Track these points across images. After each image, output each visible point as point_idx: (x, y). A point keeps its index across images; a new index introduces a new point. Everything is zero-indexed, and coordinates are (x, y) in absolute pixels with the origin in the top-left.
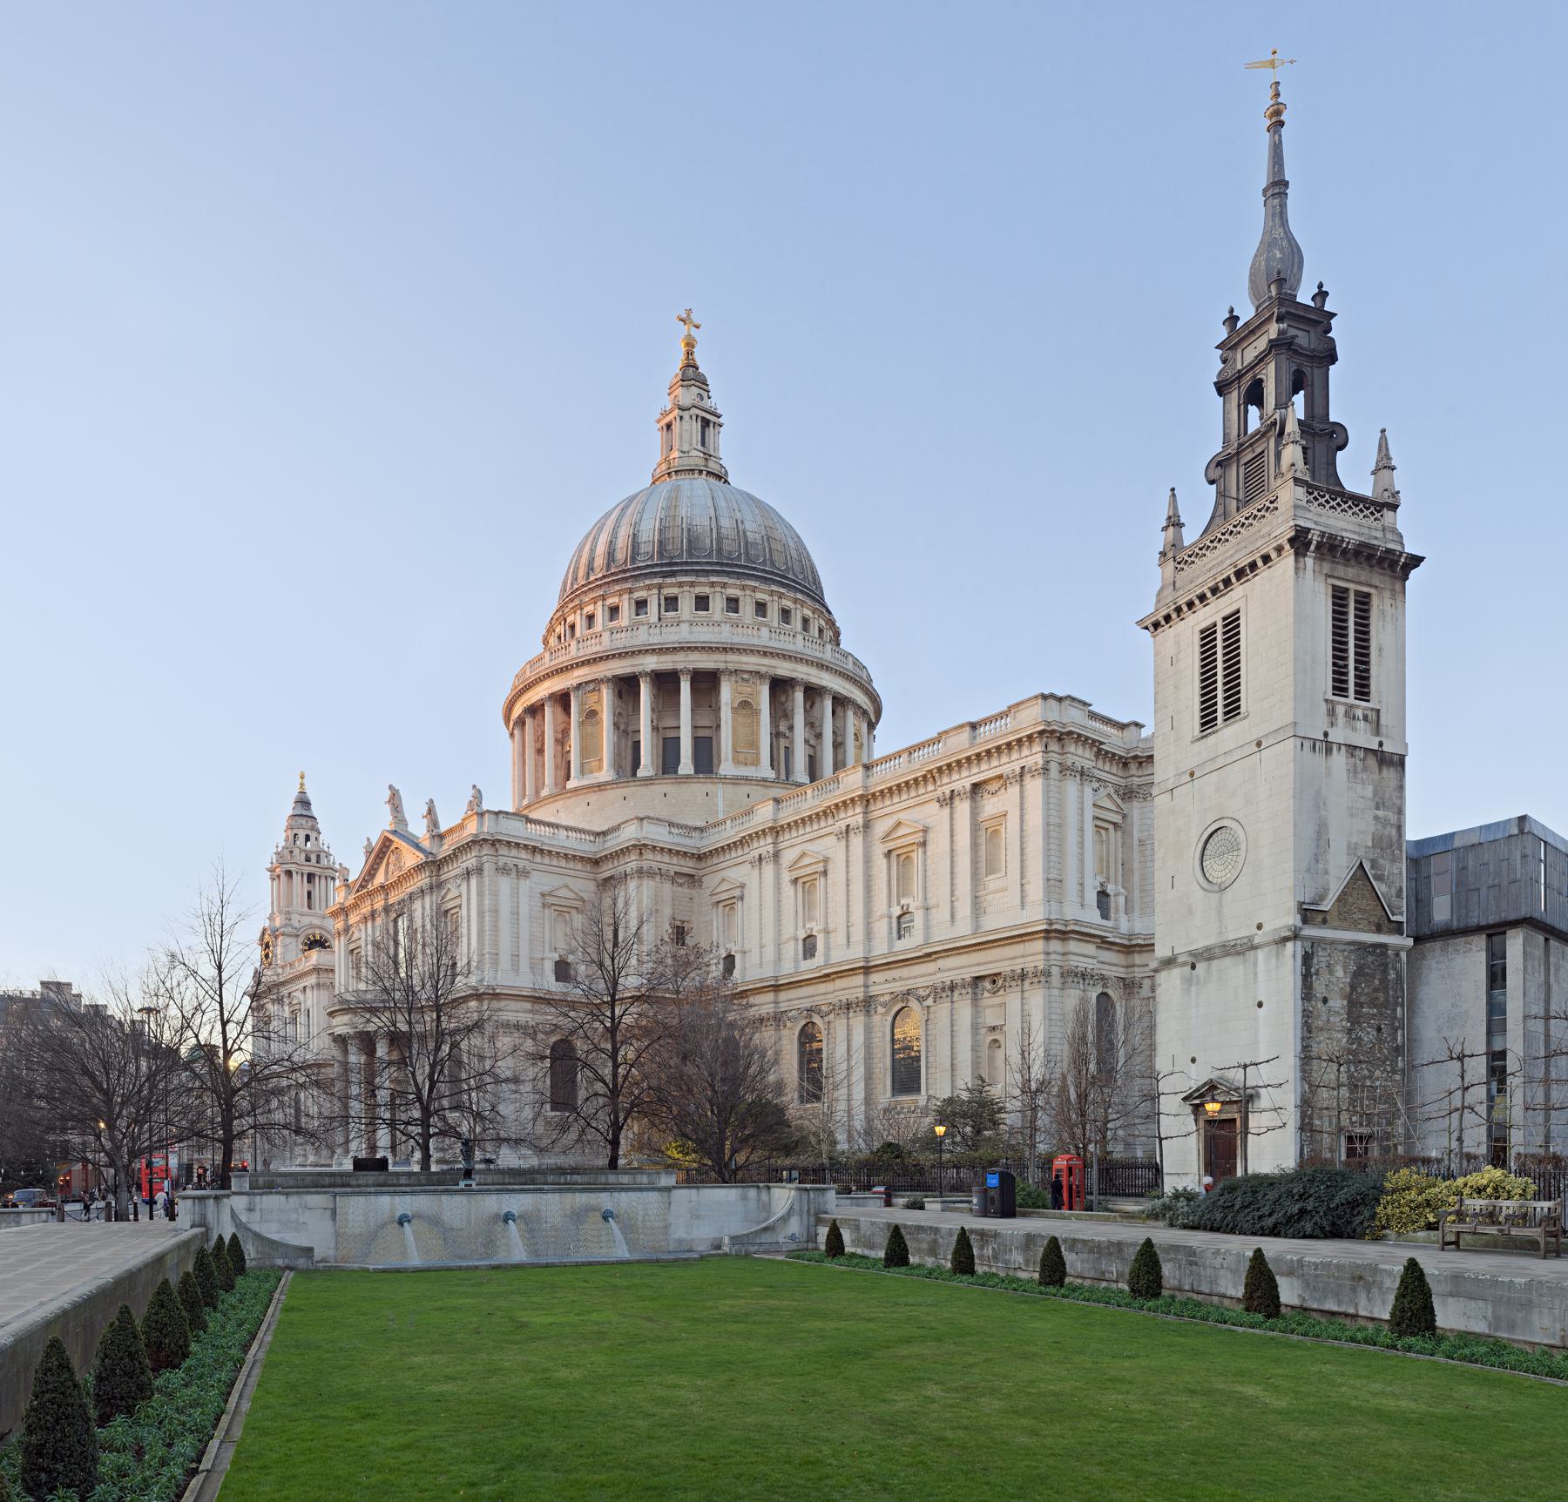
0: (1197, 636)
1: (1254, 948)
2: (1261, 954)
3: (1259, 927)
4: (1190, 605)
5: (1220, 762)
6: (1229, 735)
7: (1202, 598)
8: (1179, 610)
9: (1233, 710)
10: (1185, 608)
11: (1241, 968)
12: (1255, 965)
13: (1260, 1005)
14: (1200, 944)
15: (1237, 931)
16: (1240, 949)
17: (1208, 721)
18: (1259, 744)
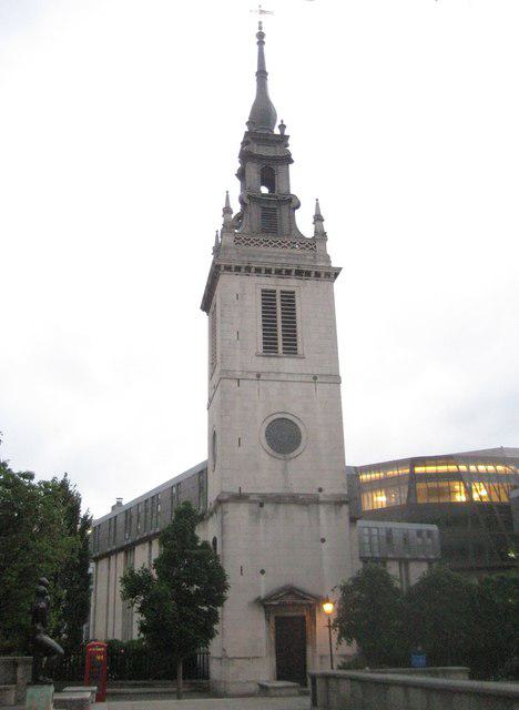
0: (259, 293)
1: (317, 502)
2: (322, 509)
3: (320, 490)
4: (258, 270)
5: (283, 377)
6: (288, 364)
7: (268, 271)
8: (248, 269)
9: (291, 348)
10: (253, 270)
11: (306, 513)
12: (318, 513)
13: (323, 540)
14: (267, 491)
15: (298, 487)
16: (308, 502)
17: (269, 346)
18: (315, 378)
